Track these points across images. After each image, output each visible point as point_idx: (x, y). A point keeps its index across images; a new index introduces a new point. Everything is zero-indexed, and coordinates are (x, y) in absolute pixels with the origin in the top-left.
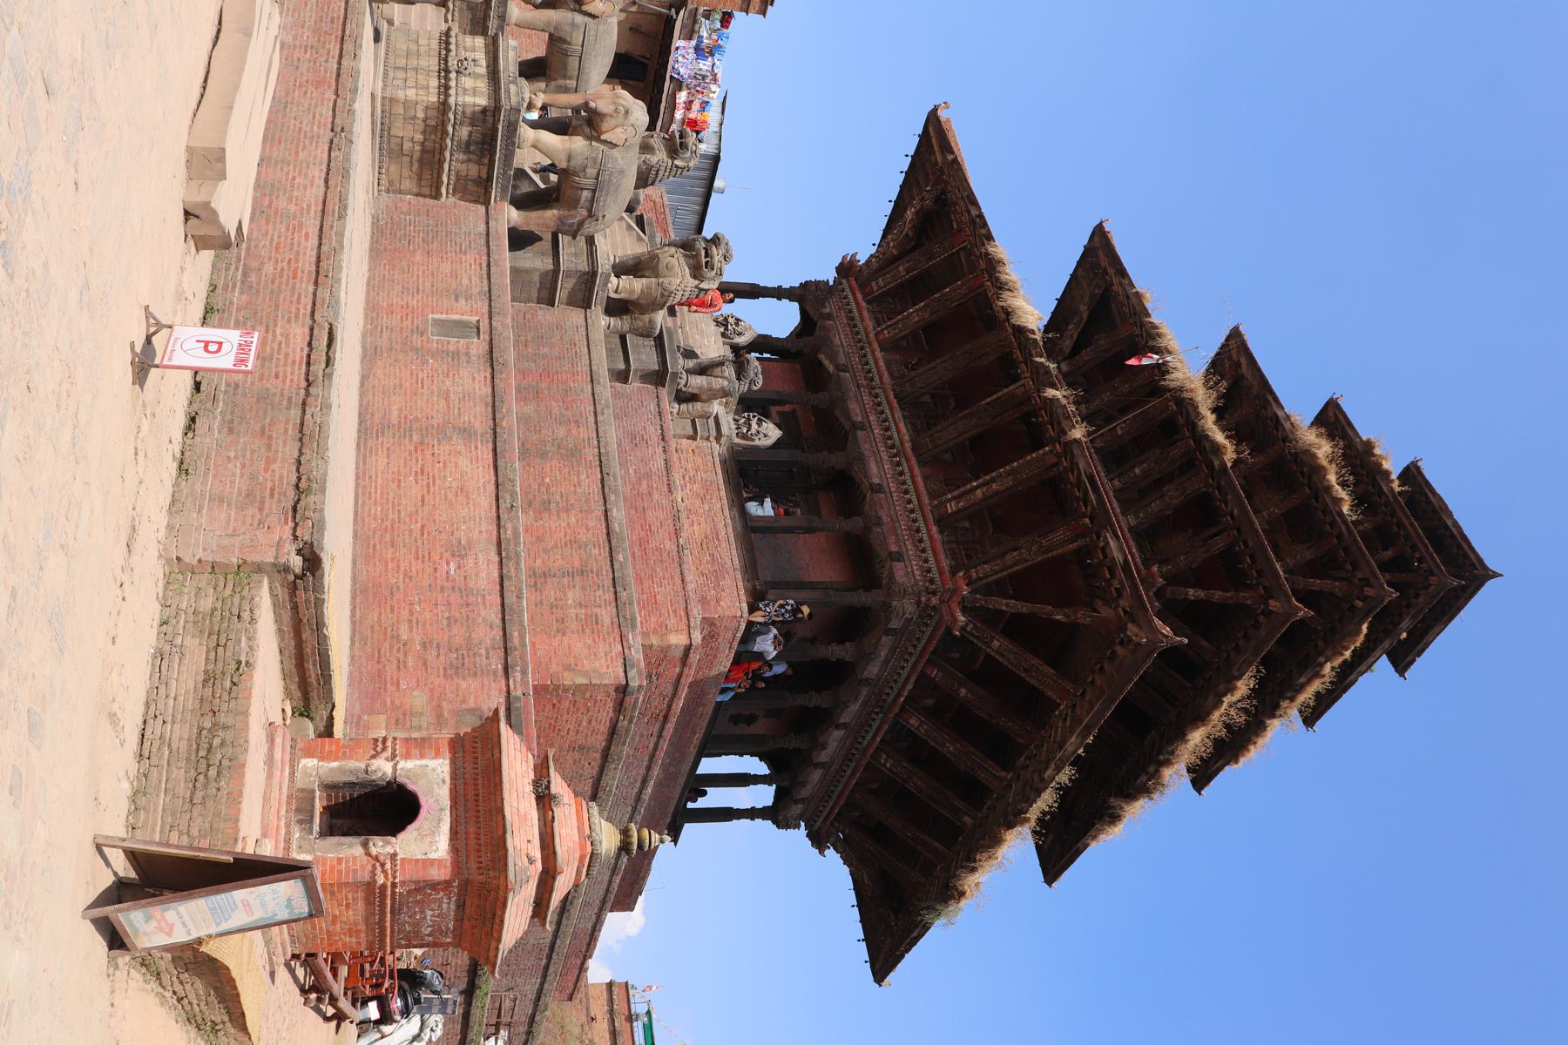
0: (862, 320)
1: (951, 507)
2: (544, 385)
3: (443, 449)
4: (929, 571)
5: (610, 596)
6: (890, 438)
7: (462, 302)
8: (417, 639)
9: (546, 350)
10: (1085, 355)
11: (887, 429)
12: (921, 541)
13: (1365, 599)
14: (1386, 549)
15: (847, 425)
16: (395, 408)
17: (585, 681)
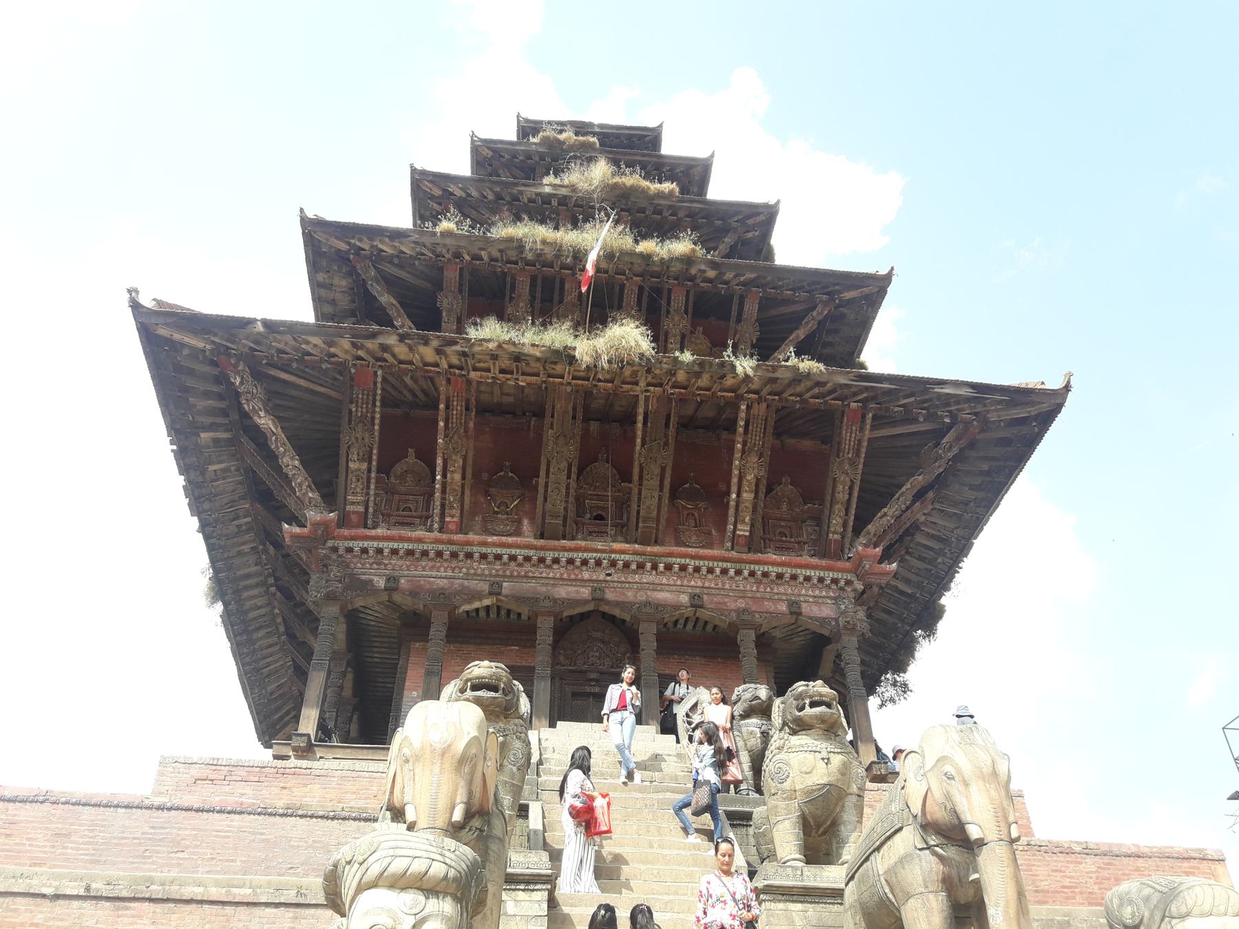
0: (420, 540)
1: (744, 530)
4: (821, 580)
6: (627, 565)
12: (780, 576)
15: (590, 607)
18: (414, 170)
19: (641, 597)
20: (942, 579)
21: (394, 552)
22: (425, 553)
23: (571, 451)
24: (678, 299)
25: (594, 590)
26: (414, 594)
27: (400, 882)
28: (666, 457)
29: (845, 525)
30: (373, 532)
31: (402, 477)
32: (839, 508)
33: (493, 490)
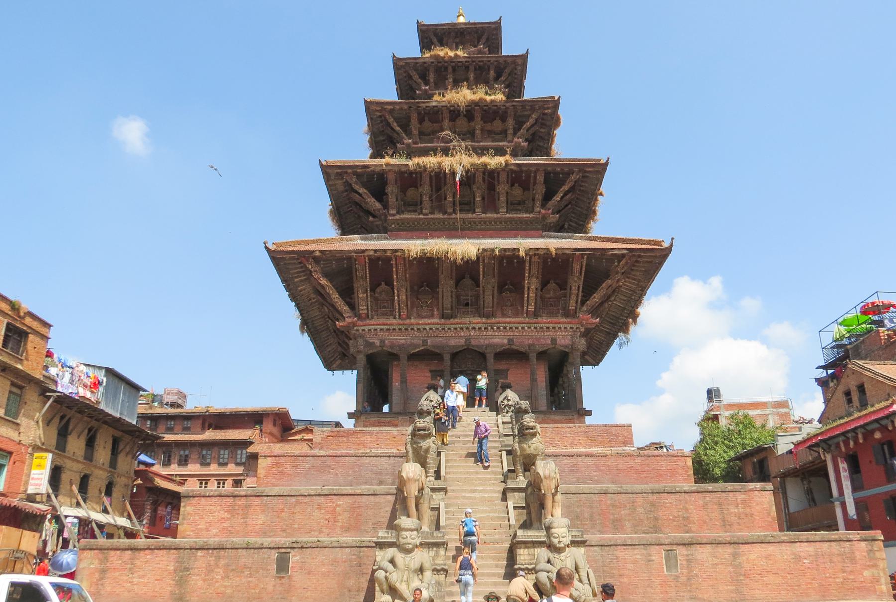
0: (392, 325)
2: (612, 517)
3: (747, 566)
4: (566, 328)
5: (731, 494)
6: (480, 328)
7: (653, 558)
8: (841, 575)
9: (586, 515)
10: (392, 199)
11: (474, 328)
12: (548, 328)
13: (548, 108)
14: (488, 73)
16: (726, 587)
17: (774, 508)
18: (366, 101)
19: (487, 342)
20: (638, 302)
21: (382, 330)
22: (394, 329)
23: (452, 282)
24: (503, 177)
25: (466, 341)
26: (392, 347)
27: (407, 530)
28: (494, 281)
29: (577, 303)
30: (372, 322)
31: (381, 293)
32: (574, 297)
33: (420, 296)
